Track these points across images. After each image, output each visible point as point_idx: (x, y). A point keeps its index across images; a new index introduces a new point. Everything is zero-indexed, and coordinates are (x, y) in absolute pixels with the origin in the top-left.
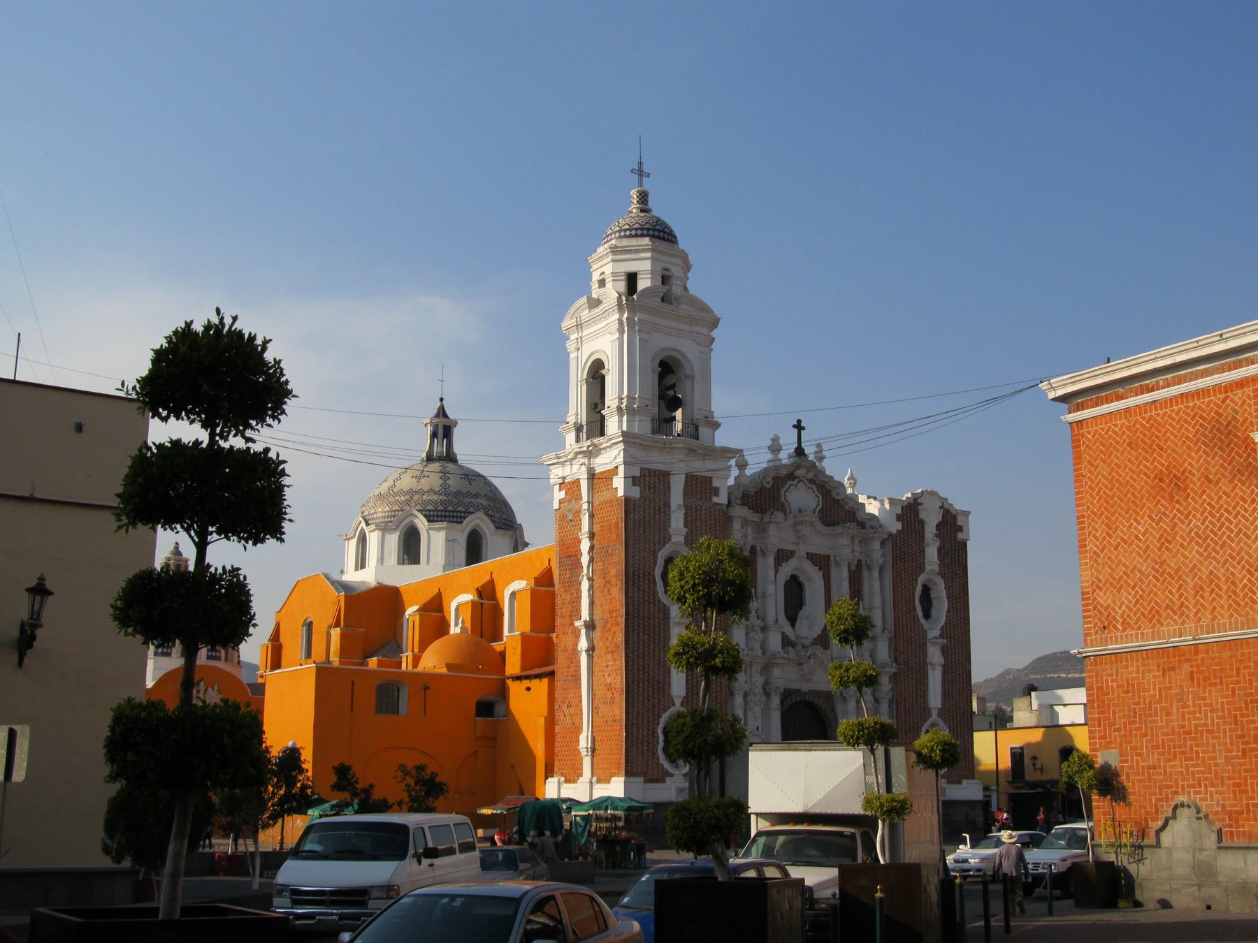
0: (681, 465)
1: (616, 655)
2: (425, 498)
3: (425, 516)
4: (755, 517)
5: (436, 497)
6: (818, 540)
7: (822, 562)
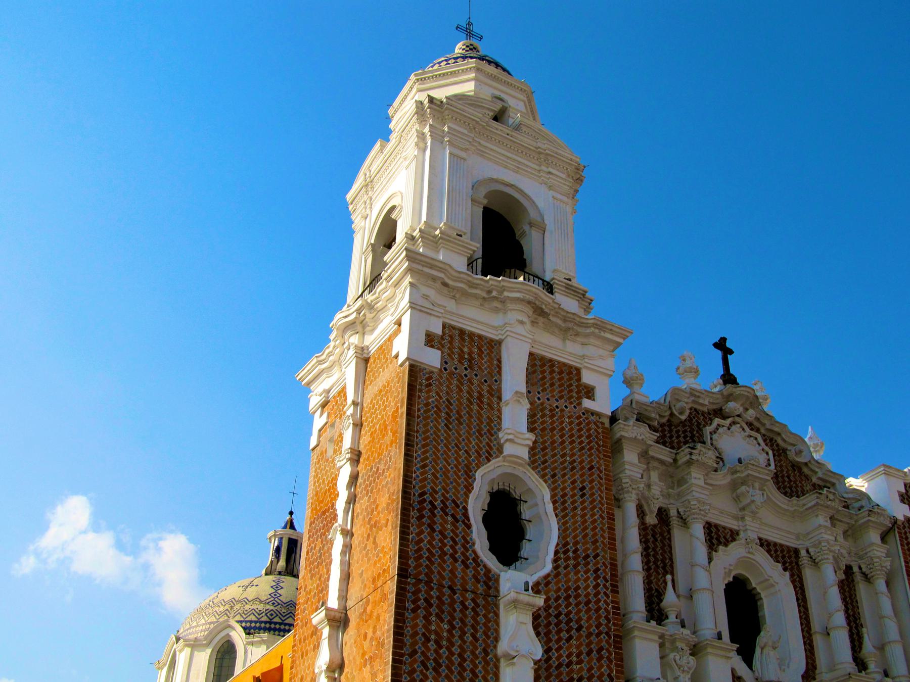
0: (520, 329)
1: (377, 664)
2: (247, 607)
3: (244, 628)
4: (663, 453)
5: (261, 607)
6: (772, 517)
7: (788, 558)
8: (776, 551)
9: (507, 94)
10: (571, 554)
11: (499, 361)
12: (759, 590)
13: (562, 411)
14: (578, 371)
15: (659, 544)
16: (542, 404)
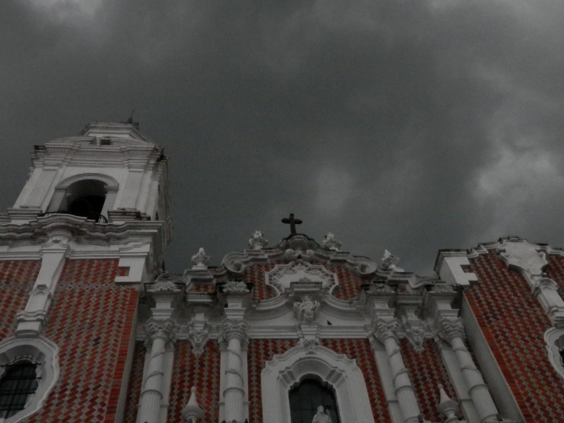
0: (56, 246)
8: (343, 346)
9: (116, 133)
10: (68, 392)
11: (38, 273)
12: (330, 383)
13: (92, 290)
14: (117, 261)
15: (206, 369)
16: (73, 290)
